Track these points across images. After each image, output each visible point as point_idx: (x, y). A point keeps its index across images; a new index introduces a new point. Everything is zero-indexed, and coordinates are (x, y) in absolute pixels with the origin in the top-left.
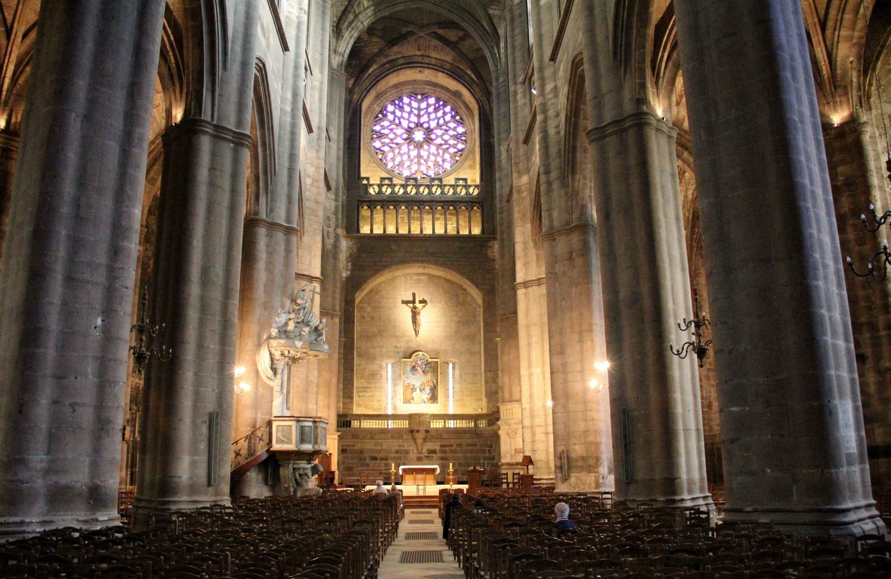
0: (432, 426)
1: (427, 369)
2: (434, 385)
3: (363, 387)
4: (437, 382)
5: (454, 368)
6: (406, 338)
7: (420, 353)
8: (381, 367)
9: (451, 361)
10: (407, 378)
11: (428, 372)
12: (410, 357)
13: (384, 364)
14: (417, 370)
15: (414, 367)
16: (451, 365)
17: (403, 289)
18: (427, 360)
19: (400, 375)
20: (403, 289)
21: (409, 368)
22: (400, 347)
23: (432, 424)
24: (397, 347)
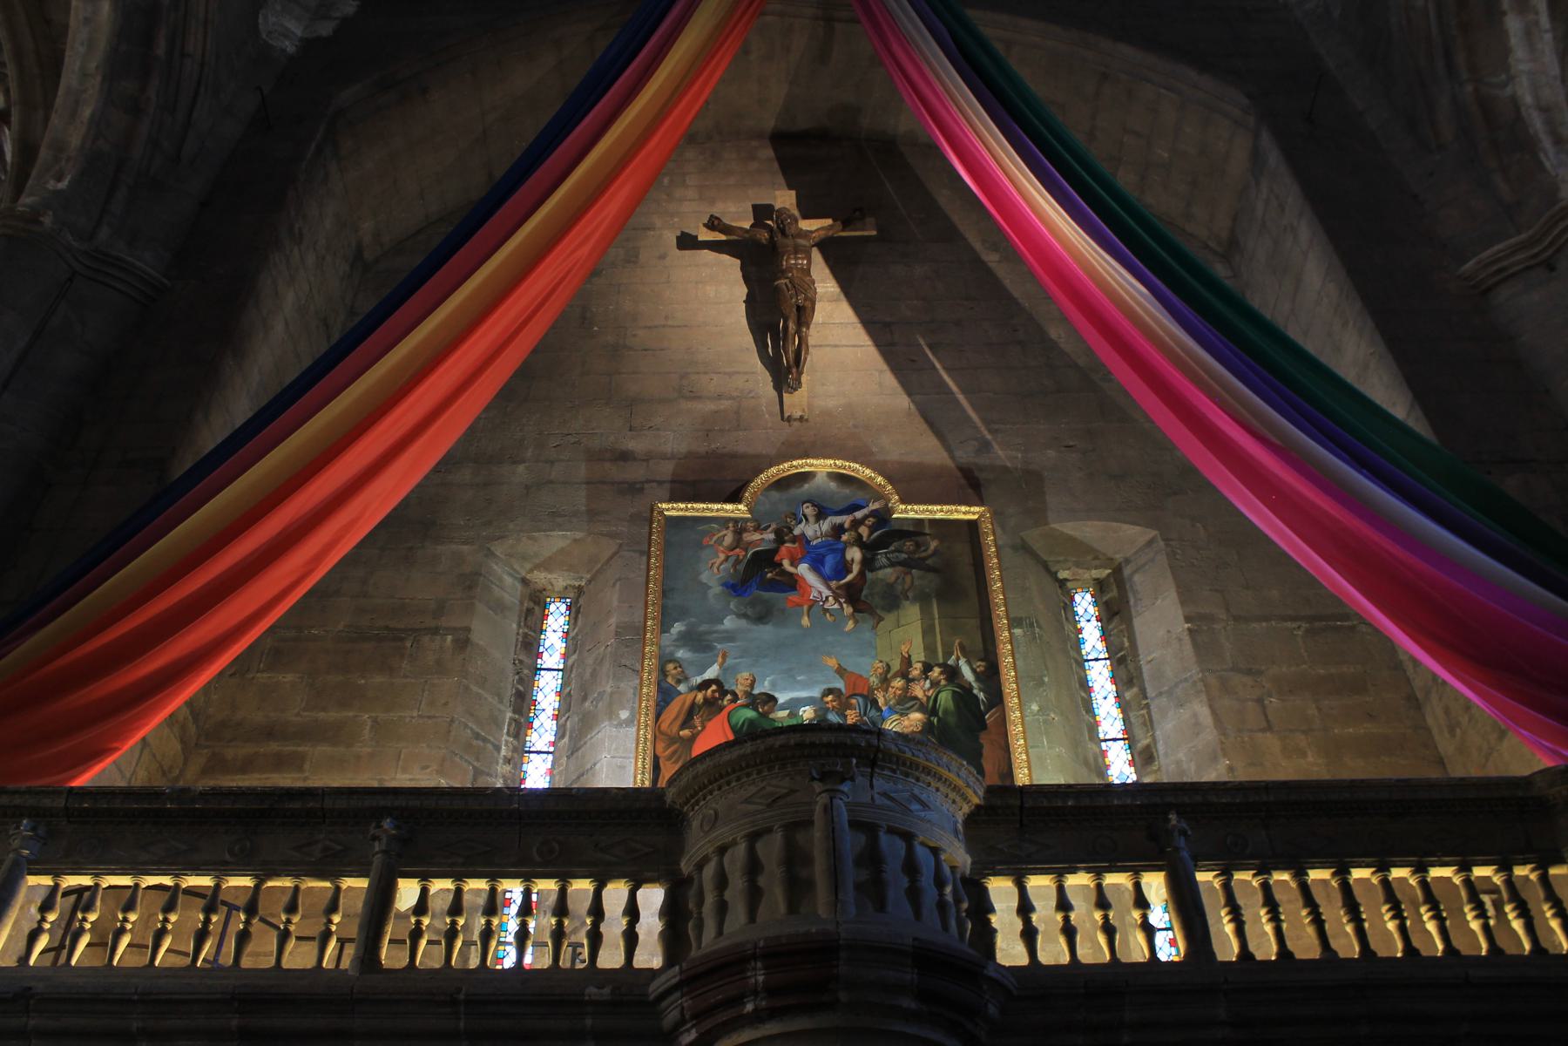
0: (1010, 952)
1: (888, 574)
2: (964, 696)
3: (270, 732)
4: (991, 675)
5: (1113, 613)
6: (711, 406)
7: (822, 466)
8: (471, 583)
9: (1082, 553)
10: (692, 639)
11: (892, 600)
12: (735, 498)
13: (507, 586)
14: (792, 583)
15: (765, 559)
16: (1084, 604)
17: (691, 193)
18: (882, 517)
19: (633, 636)
20: (691, 193)
21: (714, 569)
22: (648, 457)
23: (1004, 918)
24: (625, 456)
